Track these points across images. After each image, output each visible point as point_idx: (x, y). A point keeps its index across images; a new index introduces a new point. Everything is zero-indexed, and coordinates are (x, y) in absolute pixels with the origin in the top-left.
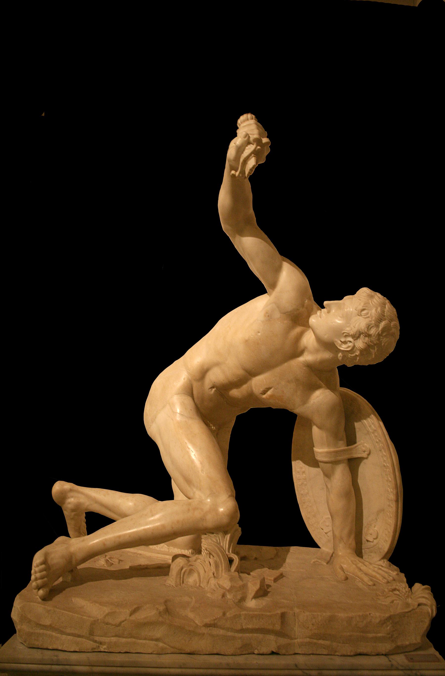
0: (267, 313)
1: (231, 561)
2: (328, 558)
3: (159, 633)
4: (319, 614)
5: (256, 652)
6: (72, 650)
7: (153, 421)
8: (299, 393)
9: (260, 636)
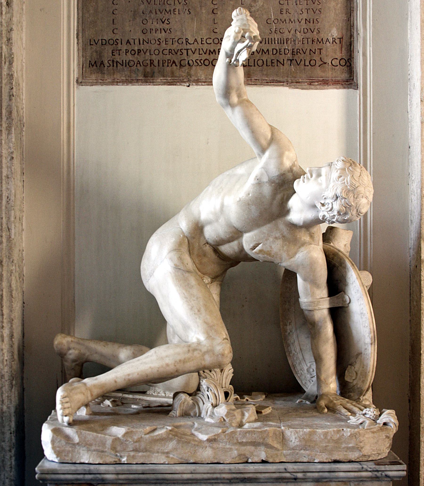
0: (256, 177)
1: (227, 394)
2: (313, 399)
3: (171, 445)
4: (301, 430)
5: (250, 461)
6: (97, 463)
7: (151, 275)
9: (253, 448)
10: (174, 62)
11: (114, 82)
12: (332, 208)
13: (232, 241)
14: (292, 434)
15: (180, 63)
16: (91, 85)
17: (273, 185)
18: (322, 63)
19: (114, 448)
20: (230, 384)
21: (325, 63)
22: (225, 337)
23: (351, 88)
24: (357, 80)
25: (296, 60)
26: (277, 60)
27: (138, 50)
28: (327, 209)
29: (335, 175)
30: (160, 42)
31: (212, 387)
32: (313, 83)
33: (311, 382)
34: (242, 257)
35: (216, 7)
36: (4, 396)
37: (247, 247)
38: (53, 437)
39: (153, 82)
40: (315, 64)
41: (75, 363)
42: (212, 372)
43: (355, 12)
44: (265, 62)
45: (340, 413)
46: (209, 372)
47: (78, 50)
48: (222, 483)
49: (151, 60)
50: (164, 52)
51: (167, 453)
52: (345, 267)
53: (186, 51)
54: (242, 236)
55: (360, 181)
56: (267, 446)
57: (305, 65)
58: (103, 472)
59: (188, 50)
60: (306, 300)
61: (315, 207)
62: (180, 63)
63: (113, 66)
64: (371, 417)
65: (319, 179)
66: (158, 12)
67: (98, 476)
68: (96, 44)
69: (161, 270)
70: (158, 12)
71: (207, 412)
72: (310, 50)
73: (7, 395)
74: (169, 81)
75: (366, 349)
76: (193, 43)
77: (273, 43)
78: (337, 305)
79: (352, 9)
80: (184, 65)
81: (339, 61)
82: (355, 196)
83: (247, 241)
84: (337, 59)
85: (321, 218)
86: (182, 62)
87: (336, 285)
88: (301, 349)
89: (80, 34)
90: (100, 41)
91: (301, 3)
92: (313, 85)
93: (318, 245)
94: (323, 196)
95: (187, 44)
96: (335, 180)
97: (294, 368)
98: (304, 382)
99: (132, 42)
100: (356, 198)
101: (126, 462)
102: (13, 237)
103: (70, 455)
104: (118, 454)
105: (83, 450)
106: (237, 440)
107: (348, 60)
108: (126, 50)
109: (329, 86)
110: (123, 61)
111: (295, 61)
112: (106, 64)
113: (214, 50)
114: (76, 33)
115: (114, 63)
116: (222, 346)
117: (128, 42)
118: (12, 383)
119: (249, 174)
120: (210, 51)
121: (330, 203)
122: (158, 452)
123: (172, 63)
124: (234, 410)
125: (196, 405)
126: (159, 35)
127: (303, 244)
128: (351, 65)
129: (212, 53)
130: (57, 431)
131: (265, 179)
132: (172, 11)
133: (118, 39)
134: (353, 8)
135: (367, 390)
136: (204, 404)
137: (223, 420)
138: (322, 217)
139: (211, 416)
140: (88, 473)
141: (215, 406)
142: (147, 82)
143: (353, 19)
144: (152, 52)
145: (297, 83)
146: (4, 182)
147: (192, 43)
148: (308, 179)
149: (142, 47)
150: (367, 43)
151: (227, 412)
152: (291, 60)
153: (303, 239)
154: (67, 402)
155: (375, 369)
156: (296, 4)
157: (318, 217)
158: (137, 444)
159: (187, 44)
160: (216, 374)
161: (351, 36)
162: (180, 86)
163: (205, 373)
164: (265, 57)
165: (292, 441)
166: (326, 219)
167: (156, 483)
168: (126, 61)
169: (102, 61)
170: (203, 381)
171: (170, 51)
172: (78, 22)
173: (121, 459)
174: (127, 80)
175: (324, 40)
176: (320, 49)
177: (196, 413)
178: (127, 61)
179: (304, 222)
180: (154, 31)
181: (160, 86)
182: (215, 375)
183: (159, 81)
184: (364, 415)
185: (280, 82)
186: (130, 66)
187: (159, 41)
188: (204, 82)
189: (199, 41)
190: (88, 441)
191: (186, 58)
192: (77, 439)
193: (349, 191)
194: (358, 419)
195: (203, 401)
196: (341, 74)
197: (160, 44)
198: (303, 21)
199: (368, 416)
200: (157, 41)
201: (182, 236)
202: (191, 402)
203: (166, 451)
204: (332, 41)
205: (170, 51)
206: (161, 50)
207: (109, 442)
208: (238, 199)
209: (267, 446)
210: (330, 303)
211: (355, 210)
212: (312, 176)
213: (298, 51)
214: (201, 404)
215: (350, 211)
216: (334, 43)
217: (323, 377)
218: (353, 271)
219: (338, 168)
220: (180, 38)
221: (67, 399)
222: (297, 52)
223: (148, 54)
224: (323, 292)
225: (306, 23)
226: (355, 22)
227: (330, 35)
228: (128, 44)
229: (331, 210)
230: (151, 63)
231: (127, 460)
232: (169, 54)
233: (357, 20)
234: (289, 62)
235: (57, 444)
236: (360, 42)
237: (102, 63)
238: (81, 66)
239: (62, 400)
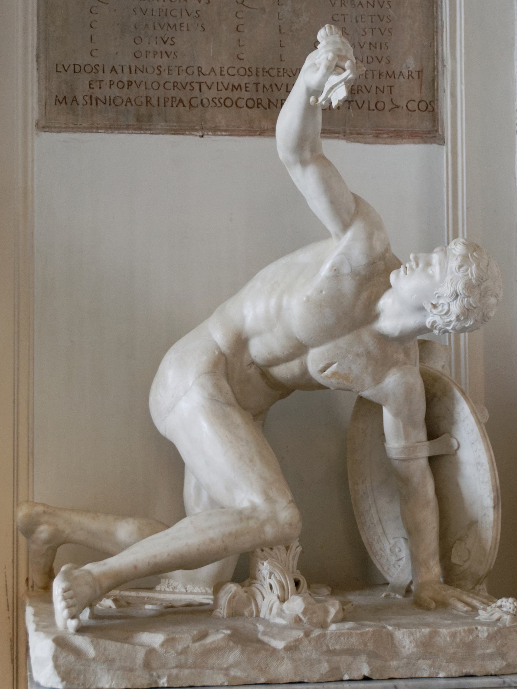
1: (297, 583)
5: (346, 677)
8: (370, 369)
9: (350, 659)
10: (181, 101)
12: (449, 311)
14: (405, 636)
15: (190, 103)
16: (58, 132)
17: (357, 278)
18: (394, 106)
19: (147, 665)
21: (398, 107)
23: (434, 143)
24: (443, 132)
25: (356, 102)
27: (128, 81)
28: (441, 311)
29: (454, 264)
30: (161, 72)
32: (381, 136)
33: (397, 566)
34: (306, 384)
35: (242, 23)
37: (313, 369)
38: (56, 651)
39: (150, 130)
40: (384, 108)
41: (48, 546)
42: (274, 550)
45: (455, 608)
46: (270, 551)
47: (39, 78)
49: (147, 97)
50: (166, 86)
51: (227, 669)
52: (452, 399)
53: (198, 85)
55: (489, 272)
57: (369, 109)
59: (202, 84)
60: (396, 445)
61: (421, 309)
62: (190, 103)
63: (91, 104)
64: (511, 611)
68: (66, 71)
69: (183, 403)
71: (271, 609)
72: (377, 87)
74: (174, 128)
75: (485, 515)
76: (209, 74)
79: (435, 29)
80: (196, 105)
81: (417, 104)
83: (314, 360)
84: (414, 101)
85: (428, 326)
86: (193, 101)
88: (380, 520)
89: (42, 55)
90: (72, 67)
91: (363, 20)
92: (382, 138)
93: (415, 365)
94: (436, 294)
95: (199, 75)
96: (454, 270)
98: (385, 568)
99: (119, 69)
100: (484, 297)
104: (155, 674)
105: (102, 669)
106: (328, 646)
107: (430, 103)
108: (110, 81)
109: (405, 140)
110: (105, 97)
111: (355, 102)
113: (239, 85)
115: (93, 100)
116: (286, 513)
117: (113, 69)
119: (320, 264)
120: (233, 86)
121: (446, 303)
122: (213, 668)
123: (177, 102)
126: (159, 61)
128: (434, 110)
129: (237, 89)
130: (61, 643)
131: (346, 270)
132: (178, 27)
133: (98, 65)
134: (437, 28)
136: (264, 598)
137: (298, 619)
138: (430, 324)
141: (283, 600)
143: (437, 44)
144: (149, 86)
145: (358, 134)
147: (208, 73)
148: (412, 269)
149: (134, 77)
151: (305, 609)
153: (394, 357)
156: (357, 22)
157: (425, 323)
158: (183, 657)
159: (199, 75)
161: (435, 69)
162: (191, 137)
163: (264, 553)
165: (404, 647)
166: (436, 327)
168: (110, 97)
169: (75, 97)
170: (263, 564)
171: (175, 84)
173: (158, 680)
176: (391, 87)
177: (253, 612)
178: (112, 98)
180: (151, 55)
181: (161, 136)
182: (278, 555)
183: (160, 127)
184: (500, 607)
185: (334, 133)
186: (117, 105)
187: (159, 70)
188: (226, 131)
189: (218, 71)
190: (109, 655)
191: (198, 96)
192: (91, 652)
194: (492, 614)
197: (160, 74)
198: (367, 46)
199: (505, 609)
200: (156, 69)
201: (217, 353)
203: (225, 666)
204: (407, 75)
205: (175, 85)
206: (162, 83)
207: (140, 655)
208: (305, 299)
212: (417, 265)
213: (360, 88)
214: (259, 598)
216: (410, 78)
219: (458, 254)
220: (190, 67)
221: (71, 593)
222: (358, 90)
223: (143, 87)
225: (370, 49)
226: (440, 49)
227: (404, 66)
228: (113, 72)
229: (446, 314)
230: (147, 101)
231: (168, 681)
232: (174, 89)
233: (442, 45)
235: (61, 661)
236: (447, 78)
238: (44, 104)
239: (65, 594)
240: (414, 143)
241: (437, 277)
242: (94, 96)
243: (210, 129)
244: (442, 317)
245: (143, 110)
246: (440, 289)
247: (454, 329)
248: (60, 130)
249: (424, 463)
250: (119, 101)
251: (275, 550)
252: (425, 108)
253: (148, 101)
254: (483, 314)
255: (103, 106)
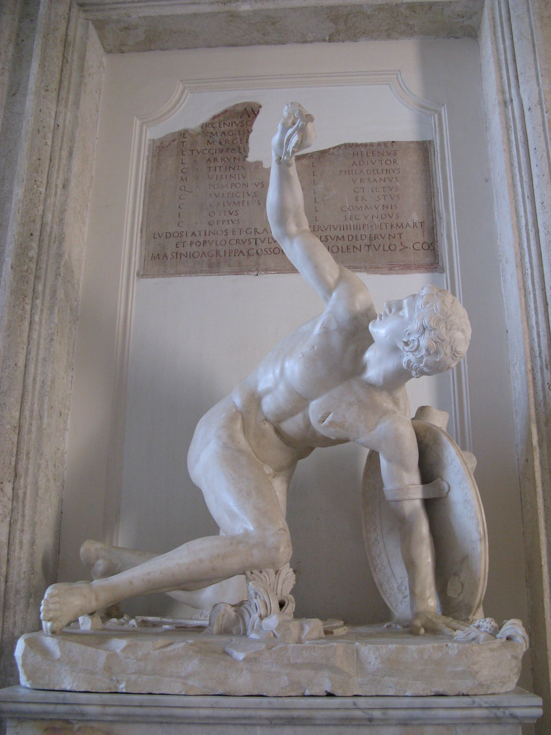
1: (282, 605)
5: (307, 693)
6: (83, 690)
10: (241, 252)
11: (178, 274)
13: (297, 413)
19: (108, 669)
20: (291, 593)
21: (406, 248)
22: (282, 526)
24: (443, 264)
26: (354, 247)
28: (412, 348)
31: (261, 592)
36: (17, 617)
37: (314, 420)
39: (218, 272)
43: (436, 197)
44: (340, 249)
46: (258, 573)
47: (141, 243)
48: (259, 725)
49: (216, 251)
51: (186, 677)
54: (307, 406)
56: (334, 669)
58: (83, 702)
64: (488, 630)
65: (401, 314)
66: (226, 204)
67: (76, 708)
70: (226, 204)
73: (21, 616)
77: (349, 229)
78: (432, 496)
82: (448, 328)
86: (250, 252)
87: (429, 470)
89: (144, 229)
94: (406, 331)
96: (420, 307)
97: (381, 587)
99: (197, 233)
100: (450, 330)
101: (124, 691)
102: (45, 426)
103: (47, 677)
104: (114, 678)
112: (169, 256)
114: (140, 227)
116: (279, 541)
118: (29, 601)
122: (171, 676)
124: (289, 621)
125: (240, 619)
127: (385, 413)
128: (434, 249)
131: (333, 326)
132: (241, 203)
134: (434, 193)
135: (478, 607)
136: (250, 616)
137: (272, 635)
139: (258, 632)
140: (61, 702)
142: (211, 273)
144: (218, 243)
146: (40, 365)
149: (207, 238)
150: (451, 226)
152: (369, 246)
154: (55, 603)
155: (487, 576)
160: (269, 575)
161: (433, 220)
163: (253, 575)
164: (340, 243)
165: (370, 663)
166: (412, 366)
167: (161, 723)
172: (143, 218)
174: (190, 271)
175: (404, 225)
176: (400, 234)
178: (192, 253)
179: (385, 378)
182: (267, 577)
188: (274, 271)
191: (254, 247)
192: (58, 653)
193: (439, 320)
194: (469, 634)
195: (247, 609)
196: (423, 257)
198: (381, 207)
201: (234, 410)
202: (233, 614)
203: (184, 674)
205: (237, 241)
209: (334, 669)
210: (424, 492)
211: (449, 347)
212: (390, 311)
213: (376, 236)
214: (247, 616)
215: (443, 348)
216: (415, 227)
217: (418, 590)
218: (451, 445)
223: (214, 244)
224: (413, 478)
226: (437, 206)
227: (410, 219)
228: (194, 236)
231: (126, 687)
233: (438, 204)
234: (367, 247)
237: (165, 256)
238: (143, 259)
240: (420, 272)
241: (407, 315)
242: (179, 252)
243: (262, 270)
244: (414, 354)
245: (214, 259)
246: (409, 327)
247: (426, 365)
248: (153, 276)
249: (418, 504)
250: (196, 254)
251: (264, 573)
252: (427, 248)
253: (217, 252)
254: (452, 347)
255: (185, 258)
